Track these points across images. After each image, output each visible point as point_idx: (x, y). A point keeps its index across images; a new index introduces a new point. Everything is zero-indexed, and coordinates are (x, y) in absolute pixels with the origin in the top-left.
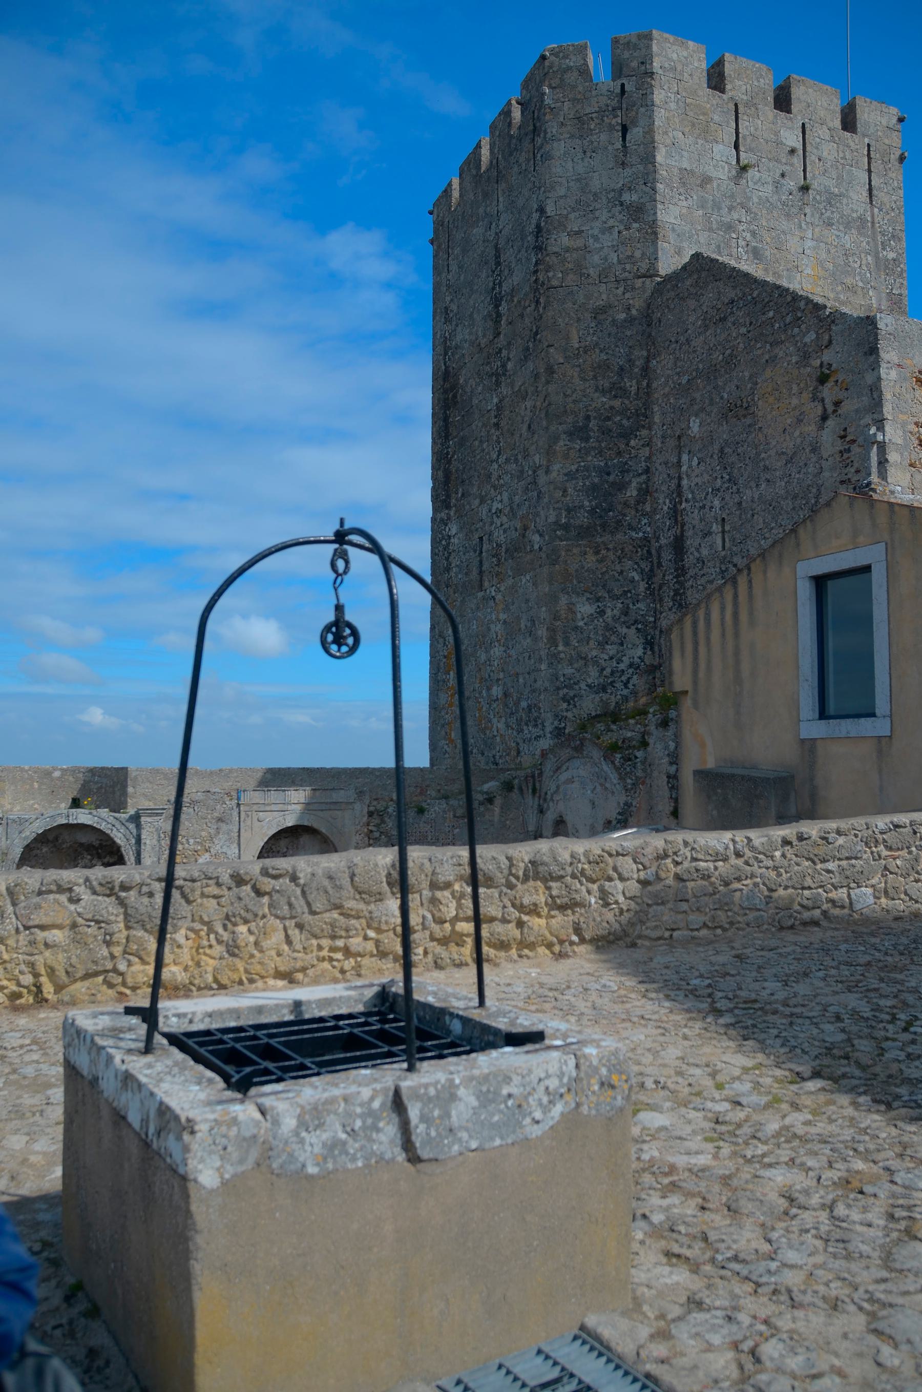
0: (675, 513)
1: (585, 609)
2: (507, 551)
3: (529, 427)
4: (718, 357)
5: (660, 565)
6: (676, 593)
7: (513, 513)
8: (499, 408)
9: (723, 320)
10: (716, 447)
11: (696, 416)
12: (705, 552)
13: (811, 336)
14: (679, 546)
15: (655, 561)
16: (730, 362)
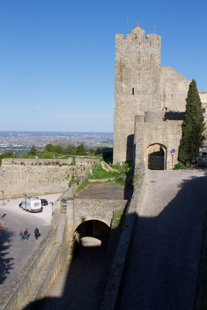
0: (164, 92)
1: (155, 100)
2: (141, 91)
3: (148, 78)
4: (172, 78)
5: (161, 97)
6: (164, 100)
7: (143, 87)
8: (139, 74)
9: (173, 75)
10: (171, 87)
11: (168, 83)
12: (169, 97)
13: (186, 81)
14: (165, 96)
15: (160, 96)
16: (174, 80)
